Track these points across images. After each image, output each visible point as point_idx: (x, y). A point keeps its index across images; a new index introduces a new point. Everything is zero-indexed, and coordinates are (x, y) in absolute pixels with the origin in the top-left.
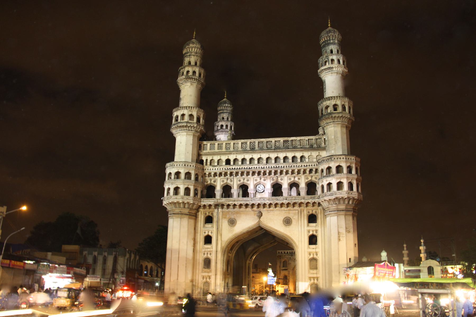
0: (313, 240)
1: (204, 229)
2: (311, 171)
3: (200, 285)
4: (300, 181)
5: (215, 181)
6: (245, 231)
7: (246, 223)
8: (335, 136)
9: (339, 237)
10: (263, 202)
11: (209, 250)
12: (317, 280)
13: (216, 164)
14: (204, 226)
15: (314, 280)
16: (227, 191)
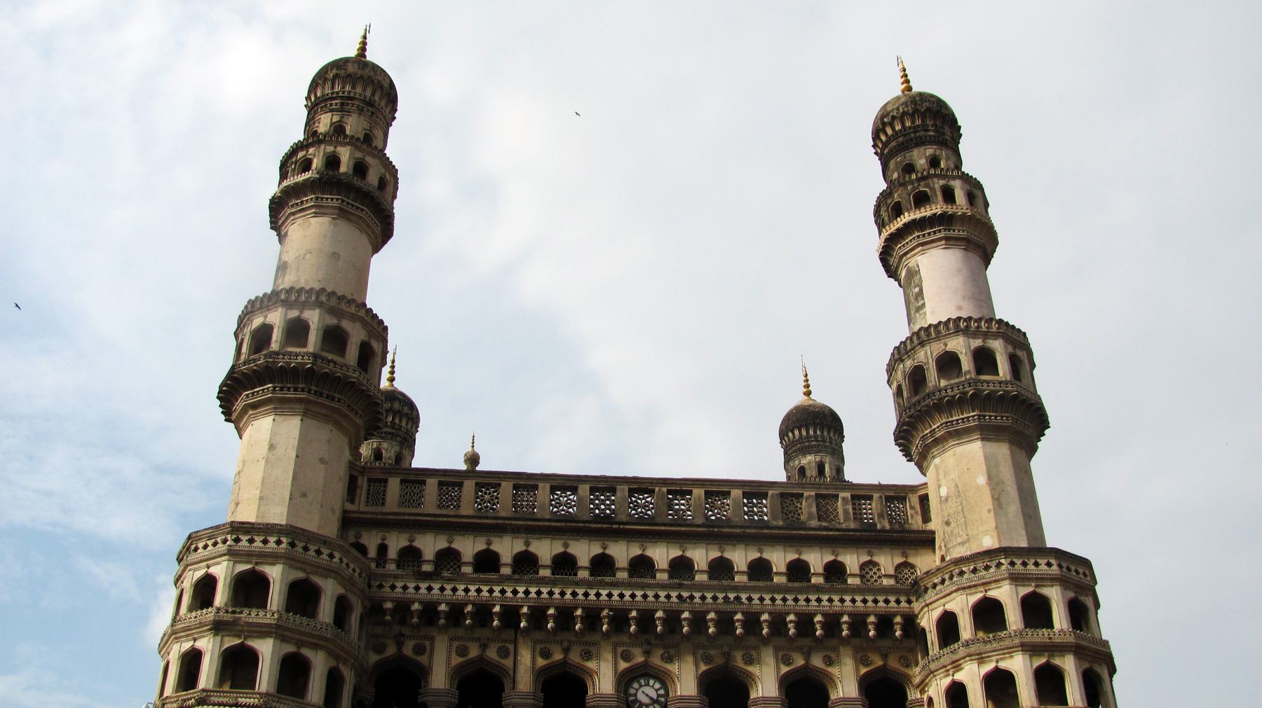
2: (885, 623)
5: (420, 650)
8: (990, 478)
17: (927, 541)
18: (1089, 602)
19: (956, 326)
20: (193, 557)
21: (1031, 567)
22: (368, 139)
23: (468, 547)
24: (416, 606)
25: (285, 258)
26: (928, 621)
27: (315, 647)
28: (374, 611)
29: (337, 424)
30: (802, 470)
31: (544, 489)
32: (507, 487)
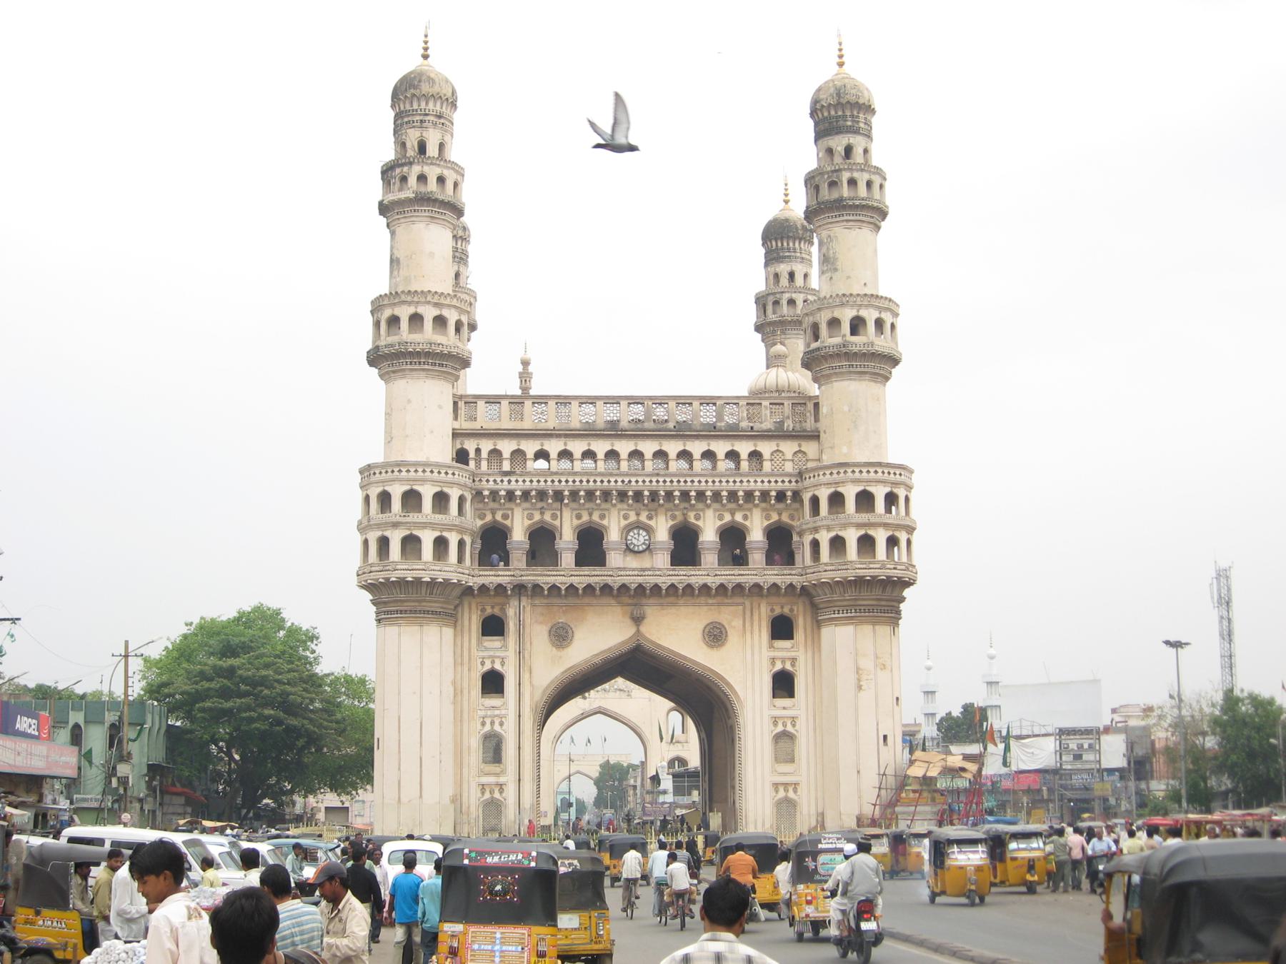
0: (783, 684)
1: (481, 654)
2: (781, 496)
3: (473, 809)
4: (748, 523)
5: (505, 517)
6: (597, 660)
7: (600, 635)
9: (859, 680)
10: (653, 580)
11: (497, 712)
12: (795, 791)
13: (506, 466)
14: (479, 643)
15: (786, 791)
16: (542, 540)
17: (815, 436)
18: (901, 493)
19: (845, 300)
20: (373, 478)
21: (864, 474)
22: (441, 146)
23: (530, 447)
24: (503, 493)
25: (397, 254)
26: (806, 497)
27: (450, 530)
28: (478, 494)
29: (445, 379)
30: (777, 276)
31: (575, 404)
32: (552, 403)
